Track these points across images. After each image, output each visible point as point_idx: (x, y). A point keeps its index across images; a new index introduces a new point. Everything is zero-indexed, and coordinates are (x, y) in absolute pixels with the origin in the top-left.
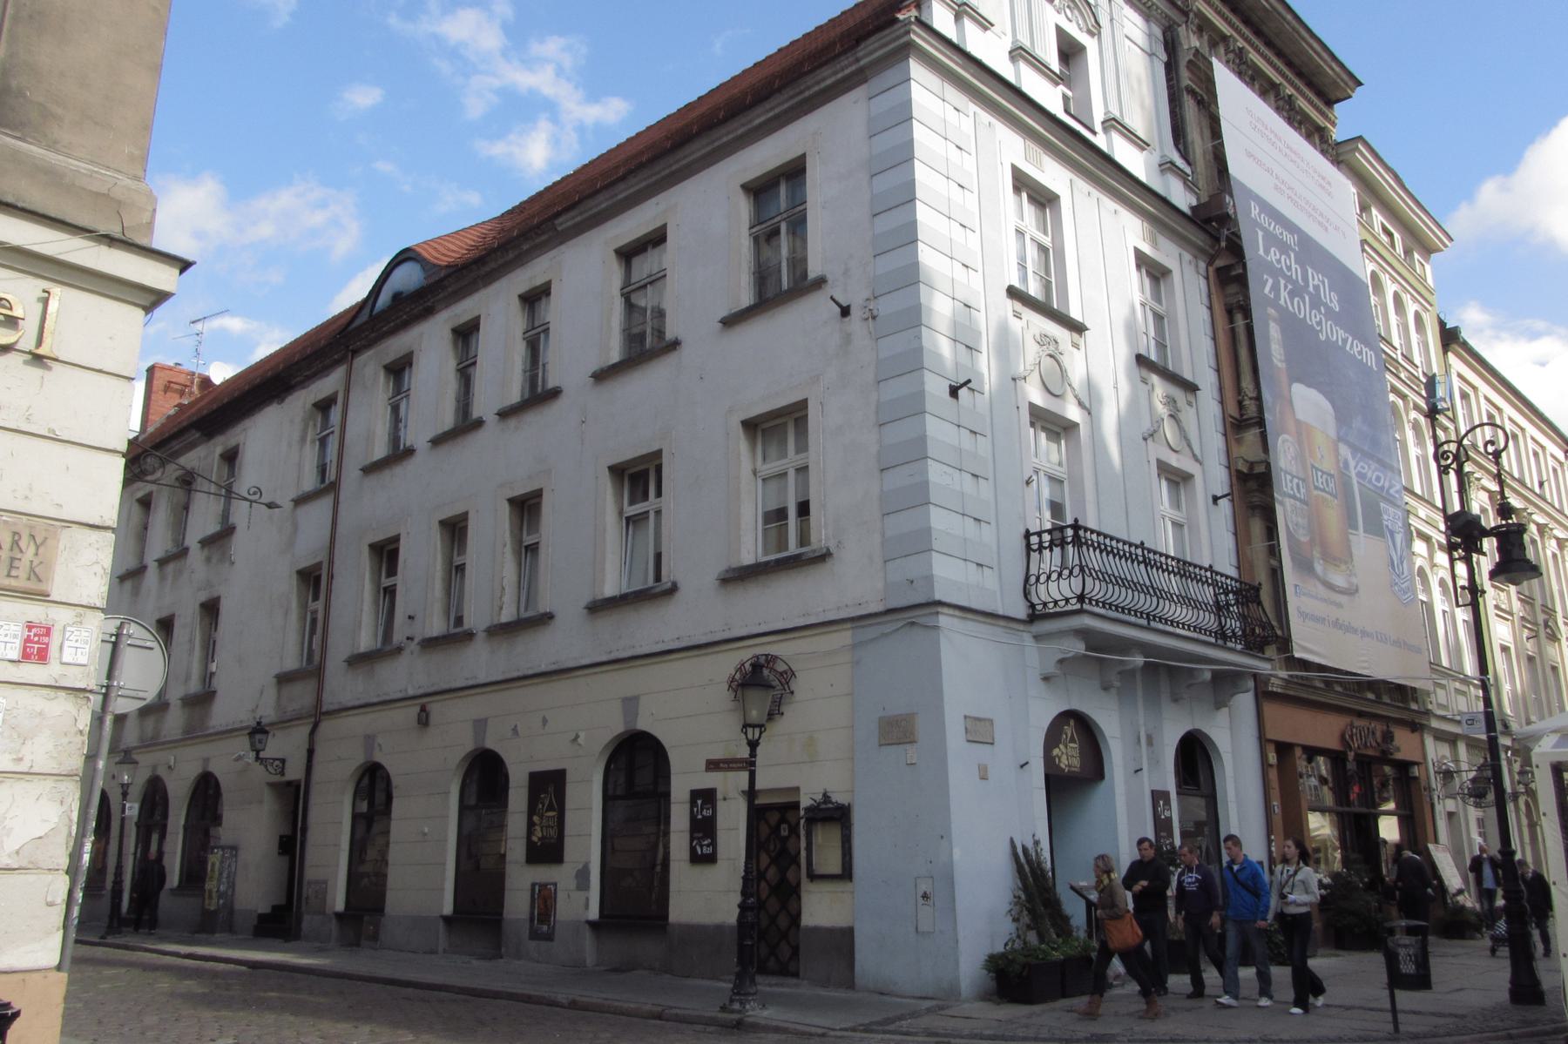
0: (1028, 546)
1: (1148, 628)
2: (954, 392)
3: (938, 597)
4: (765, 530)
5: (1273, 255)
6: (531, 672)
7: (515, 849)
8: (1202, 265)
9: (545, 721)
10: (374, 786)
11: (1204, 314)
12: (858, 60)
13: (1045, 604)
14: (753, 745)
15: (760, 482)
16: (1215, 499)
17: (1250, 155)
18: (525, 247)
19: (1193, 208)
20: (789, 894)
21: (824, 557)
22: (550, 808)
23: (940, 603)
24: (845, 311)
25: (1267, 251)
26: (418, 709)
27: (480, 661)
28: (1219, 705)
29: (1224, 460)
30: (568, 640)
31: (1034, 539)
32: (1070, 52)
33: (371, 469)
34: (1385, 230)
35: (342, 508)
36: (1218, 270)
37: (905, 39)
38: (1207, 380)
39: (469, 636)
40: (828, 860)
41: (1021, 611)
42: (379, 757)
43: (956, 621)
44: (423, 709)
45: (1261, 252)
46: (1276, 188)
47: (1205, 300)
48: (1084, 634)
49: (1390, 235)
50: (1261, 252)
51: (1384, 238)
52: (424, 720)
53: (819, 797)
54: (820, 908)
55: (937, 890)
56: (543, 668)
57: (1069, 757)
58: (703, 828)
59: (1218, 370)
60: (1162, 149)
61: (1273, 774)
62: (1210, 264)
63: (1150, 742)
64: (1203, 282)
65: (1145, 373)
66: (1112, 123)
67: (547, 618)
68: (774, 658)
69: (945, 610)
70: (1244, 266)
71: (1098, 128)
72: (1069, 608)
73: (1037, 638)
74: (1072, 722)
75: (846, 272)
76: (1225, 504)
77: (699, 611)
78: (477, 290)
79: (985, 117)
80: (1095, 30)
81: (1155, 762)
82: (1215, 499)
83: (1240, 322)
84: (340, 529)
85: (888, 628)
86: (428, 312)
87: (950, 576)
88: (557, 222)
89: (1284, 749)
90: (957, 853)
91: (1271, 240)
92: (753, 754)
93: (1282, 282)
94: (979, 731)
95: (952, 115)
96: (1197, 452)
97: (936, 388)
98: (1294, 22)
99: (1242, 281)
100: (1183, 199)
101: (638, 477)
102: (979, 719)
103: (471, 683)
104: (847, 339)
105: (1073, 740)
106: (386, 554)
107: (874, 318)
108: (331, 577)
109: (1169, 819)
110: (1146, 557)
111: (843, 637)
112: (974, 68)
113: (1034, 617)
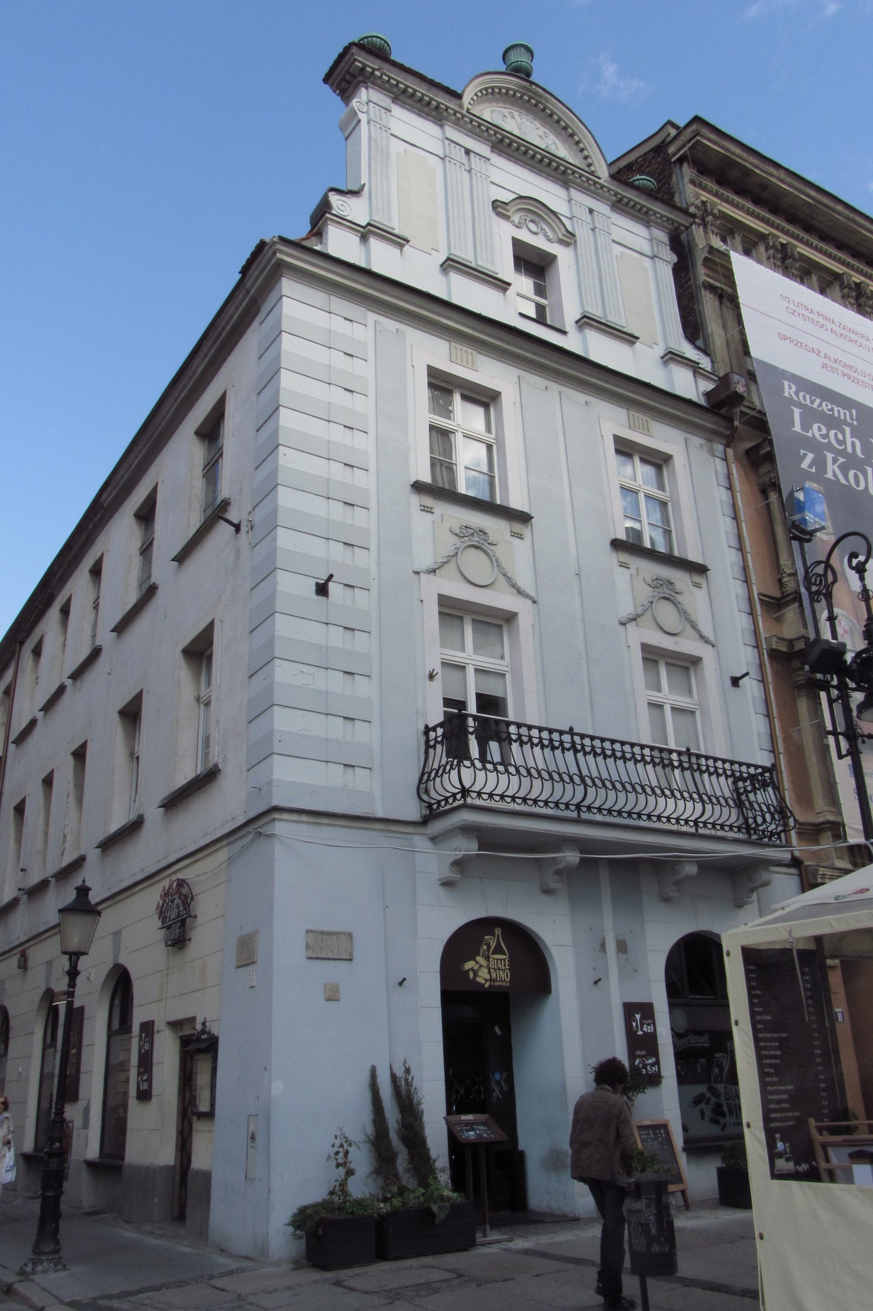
0: (427, 741)
1: (578, 821)
2: (322, 590)
3: (275, 802)
5: (816, 431)
8: (719, 448)
11: (723, 495)
12: (248, 291)
13: (439, 802)
15: (202, 706)
16: (735, 682)
17: (784, 338)
18: (90, 527)
19: (708, 395)
24: (237, 528)
25: (806, 426)
29: (750, 640)
31: (432, 735)
36: (748, 452)
38: (724, 563)
41: (412, 811)
43: (303, 827)
45: (797, 428)
46: (825, 366)
47: (724, 482)
48: (467, 830)
50: (797, 428)
57: (488, 969)
59: (741, 549)
60: (666, 341)
62: (727, 445)
63: (622, 947)
64: (720, 465)
65: (625, 557)
66: (586, 321)
68: (181, 883)
69: (286, 816)
70: (771, 442)
71: (569, 324)
72: (457, 803)
73: (434, 839)
74: (498, 931)
75: (241, 491)
76: (751, 687)
79: (390, 324)
80: (569, 239)
82: (735, 682)
83: (773, 497)
87: (294, 778)
90: (277, 1087)
91: (810, 416)
92: (72, 984)
93: (830, 456)
94: (329, 946)
95: (338, 325)
96: (707, 631)
97: (293, 586)
98: (847, 212)
99: (770, 457)
100: (686, 385)
105: (498, 950)
107: (252, 529)
112: (363, 279)
113: (432, 813)
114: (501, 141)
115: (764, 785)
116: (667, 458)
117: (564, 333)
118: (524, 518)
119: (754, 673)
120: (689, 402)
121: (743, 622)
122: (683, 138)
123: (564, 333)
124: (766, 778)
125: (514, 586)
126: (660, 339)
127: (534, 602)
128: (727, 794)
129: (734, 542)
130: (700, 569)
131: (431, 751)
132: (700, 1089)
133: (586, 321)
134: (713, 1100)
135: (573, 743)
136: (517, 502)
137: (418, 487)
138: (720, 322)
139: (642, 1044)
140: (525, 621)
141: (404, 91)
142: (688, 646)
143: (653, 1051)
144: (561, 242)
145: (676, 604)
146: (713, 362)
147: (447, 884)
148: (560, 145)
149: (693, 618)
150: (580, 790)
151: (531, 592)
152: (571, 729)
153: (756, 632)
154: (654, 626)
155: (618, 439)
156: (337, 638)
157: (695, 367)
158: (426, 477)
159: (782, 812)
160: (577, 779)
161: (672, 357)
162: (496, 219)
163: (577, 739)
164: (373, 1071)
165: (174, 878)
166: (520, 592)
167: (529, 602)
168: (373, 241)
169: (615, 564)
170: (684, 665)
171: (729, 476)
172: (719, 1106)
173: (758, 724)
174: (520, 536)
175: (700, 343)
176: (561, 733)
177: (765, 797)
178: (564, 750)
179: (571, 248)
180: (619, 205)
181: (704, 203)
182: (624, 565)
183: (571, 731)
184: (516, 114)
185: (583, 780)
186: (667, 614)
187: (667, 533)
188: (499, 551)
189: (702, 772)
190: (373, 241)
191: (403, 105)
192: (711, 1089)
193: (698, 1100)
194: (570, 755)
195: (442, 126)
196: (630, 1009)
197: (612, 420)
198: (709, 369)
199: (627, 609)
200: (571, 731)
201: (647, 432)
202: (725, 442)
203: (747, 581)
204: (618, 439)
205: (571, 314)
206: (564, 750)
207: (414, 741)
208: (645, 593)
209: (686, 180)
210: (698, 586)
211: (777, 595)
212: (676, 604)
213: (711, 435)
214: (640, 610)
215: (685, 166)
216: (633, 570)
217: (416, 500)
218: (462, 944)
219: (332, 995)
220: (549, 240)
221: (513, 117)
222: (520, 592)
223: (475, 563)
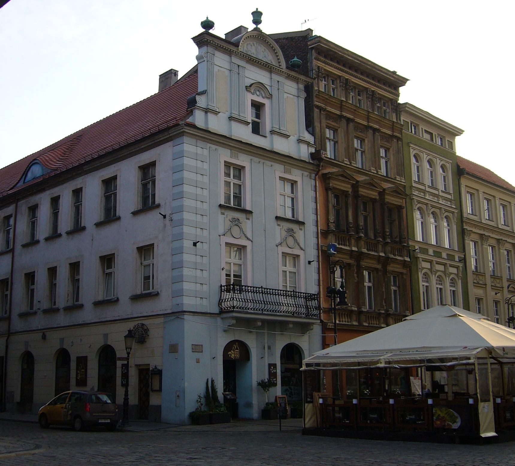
0: (221, 289)
1: (262, 314)
2: (195, 244)
4: (144, 282)
6: (77, 323)
7: (73, 381)
9: (81, 340)
10: (28, 359)
11: (313, 193)
12: (170, 134)
14: (128, 354)
16: (309, 262)
19: (312, 154)
20: (147, 395)
21: (157, 294)
22: (83, 369)
23: (185, 312)
24: (165, 217)
26: (42, 334)
27: (62, 319)
29: (316, 247)
30: (88, 314)
32: (258, 107)
33: (25, 246)
35: (16, 258)
37: (182, 130)
39: (58, 310)
40: (156, 386)
41: (216, 310)
42: (30, 349)
43: (191, 316)
44: (44, 334)
47: (313, 188)
49: (431, 134)
51: (427, 137)
52: (44, 337)
53: (154, 367)
54: (154, 400)
55: (180, 395)
56: (80, 322)
57: (234, 354)
58: (126, 376)
62: (316, 175)
63: (269, 348)
64: (313, 182)
65: (279, 223)
66: (272, 132)
67: (81, 306)
68: (143, 325)
71: (268, 134)
73: (222, 318)
74: (237, 343)
75: (165, 203)
76: (314, 265)
77: (125, 308)
78: (59, 185)
79: (214, 147)
81: (271, 354)
82: (309, 262)
84: (15, 267)
85: (173, 318)
86: (42, 190)
87: (189, 302)
88: (84, 167)
90: (186, 384)
92: (128, 356)
94: (197, 348)
95: (199, 151)
96: (302, 245)
97: (187, 244)
101: (108, 261)
102: (197, 345)
103: (59, 326)
104: (165, 226)
105: (237, 349)
106: (30, 277)
108: (12, 283)
111: (161, 320)
113: (222, 312)
114: (250, 60)
116: (296, 182)
117: (266, 137)
118: (251, 212)
119: (316, 259)
122: (313, 41)
123: (266, 137)
126: (297, 134)
128: (304, 304)
131: (223, 293)
133: (272, 132)
136: (248, 208)
137: (220, 206)
139: (273, 375)
140: (249, 249)
141: (220, 46)
142: (297, 251)
144: (267, 98)
145: (294, 237)
146: (315, 138)
147: (225, 331)
148: (269, 54)
151: (251, 239)
156: (199, 259)
157: (308, 144)
158: (223, 203)
159: (319, 308)
160: (263, 302)
161: (300, 141)
162: (246, 92)
163: (263, 290)
164: (208, 380)
165: (139, 322)
166: (248, 239)
168: (209, 114)
171: (316, 186)
173: (314, 276)
174: (248, 219)
176: (259, 288)
177: (314, 303)
178: (260, 293)
179: (270, 100)
180: (288, 77)
181: (319, 67)
182: (279, 225)
183: (262, 287)
184: (255, 43)
186: (290, 241)
188: (242, 226)
189: (297, 297)
190: (209, 115)
191: (219, 51)
193: (286, 390)
195: (231, 56)
196: (270, 365)
197: (279, 170)
199: (278, 241)
200: (262, 287)
203: (317, 226)
205: (268, 128)
206: (260, 293)
207: (217, 289)
208: (284, 234)
209: (313, 57)
210: (301, 229)
212: (294, 237)
215: (313, 51)
216: (281, 227)
217: (219, 211)
218: (228, 348)
219: (198, 361)
220: (263, 97)
221: (254, 45)
222: (248, 239)
223: (236, 231)
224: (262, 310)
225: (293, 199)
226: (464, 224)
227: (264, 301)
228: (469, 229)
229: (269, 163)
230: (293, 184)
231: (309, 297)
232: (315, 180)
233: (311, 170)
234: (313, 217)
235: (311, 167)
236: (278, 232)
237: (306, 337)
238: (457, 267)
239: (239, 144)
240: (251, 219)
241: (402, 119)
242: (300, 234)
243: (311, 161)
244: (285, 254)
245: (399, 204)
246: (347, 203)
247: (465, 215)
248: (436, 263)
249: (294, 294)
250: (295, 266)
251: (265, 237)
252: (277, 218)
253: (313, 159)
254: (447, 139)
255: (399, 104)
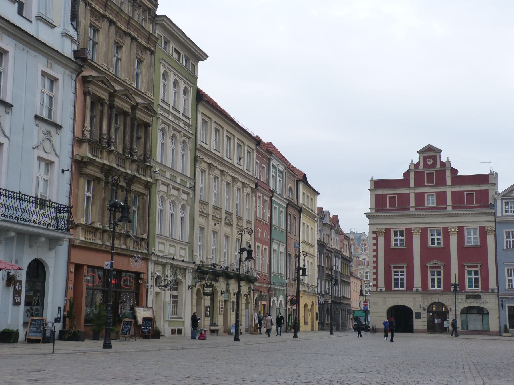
8: (74, 76)
11: (72, 96)
19: (74, 52)
28: (50, 249)
29: (70, 156)
34: (176, 50)
38: (67, 124)
47: (73, 90)
49: (179, 53)
51: (175, 56)
60: (64, 26)
61: (72, 276)
62: (77, 76)
64: (73, 83)
65: (38, 122)
66: (40, 18)
71: (33, 19)
76: (67, 174)
82: (63, 171)
89: (78, 267)
96: (58, 153)
109: (21, 291)
110: (21, 197)
115: (67, 212)
116: (57, 79)
117: (31, 22)
120: (69, 59)
121: (70, 148)
123: (31, 22)
124: (68, 209)
125: (4, 133)
126: (62, 25)
127: (9, 139)
129: (72, 117)
130: (59, 127)
132: (29, 308)
134: (31, 311)
135: (20, 197)
138: (84, 16)
142: (51, 157)
143: (20, 295)
149: (54, 147)
150: (21, 213)
151: (8, 136)
152: (20, 192)
153: (73, 152)
154: (43, 150)
155: (43, 72)
157: (72, 39)
160: (20, 210)
161: (65, 35)
166: (6, 136)
167: (7, 139)
169: (35, 125)
170: (49, 163)
171: (76, 88)
172: (32, 313)
175: (74, 23)
176: (17, 193)
177: (64, 216)
178: (17, 199)
185: (22, 211)
186: (47, 144)
187: (50, 110)
192: (31, 308)
194: (18, 201)
197: (41, 64)
198: (76, 39)
199: (35, 143)
201: (52, 68)
202: (77, 74)
203: (73, 132)
204: (43, 72)
206: (17, 199)
208: (42, 136)
211: (81, 138)
213: (73, 71)
214: (39, 143)
222: (6, 136)
224: (18, 218)
225: (51, 98)
226: (197, 152)
227: (21, 209)
228: (201, 157)
229: (33, 53)
230: (53, 80)
231: (59, 209)
232: (76, 81)
233: (74, 69)
234: (71, 122)
235: (73, 66)
236: (37, 133)
237: (52, 253)
238: (188, 194)
239: (6, 24)
240: (10, 114)
241: (157, 32)
242: (56, 139)
243: (73, 59)
244: (40, 159)
245: (148, 121)
246: (102, 112)
247: (199, 142)
248: (173, 188)
249: (43, 203)
250: (47, 173)
251: (23, 136)
252: (36, 117)
253: (76, 58)
254: (191, 62)
255: (156, 15)
